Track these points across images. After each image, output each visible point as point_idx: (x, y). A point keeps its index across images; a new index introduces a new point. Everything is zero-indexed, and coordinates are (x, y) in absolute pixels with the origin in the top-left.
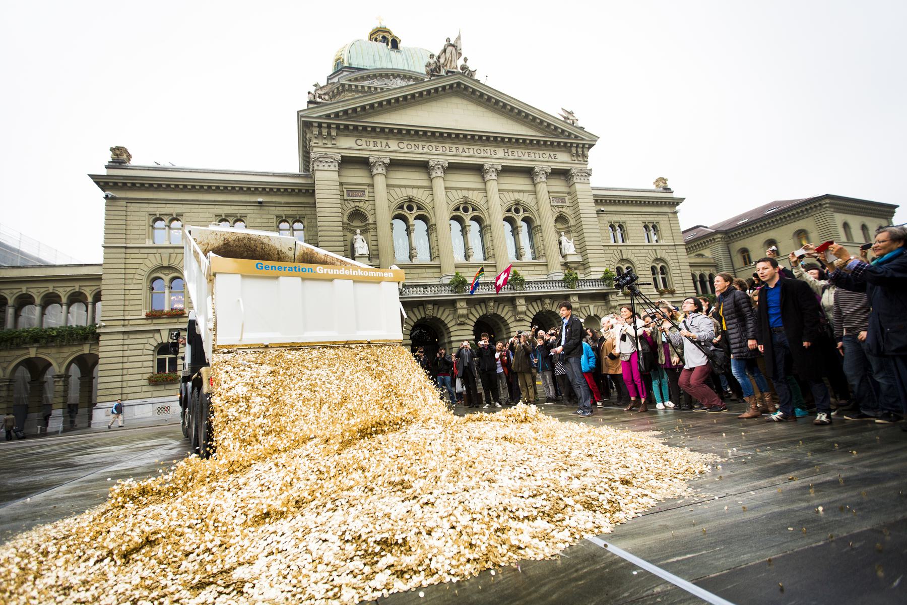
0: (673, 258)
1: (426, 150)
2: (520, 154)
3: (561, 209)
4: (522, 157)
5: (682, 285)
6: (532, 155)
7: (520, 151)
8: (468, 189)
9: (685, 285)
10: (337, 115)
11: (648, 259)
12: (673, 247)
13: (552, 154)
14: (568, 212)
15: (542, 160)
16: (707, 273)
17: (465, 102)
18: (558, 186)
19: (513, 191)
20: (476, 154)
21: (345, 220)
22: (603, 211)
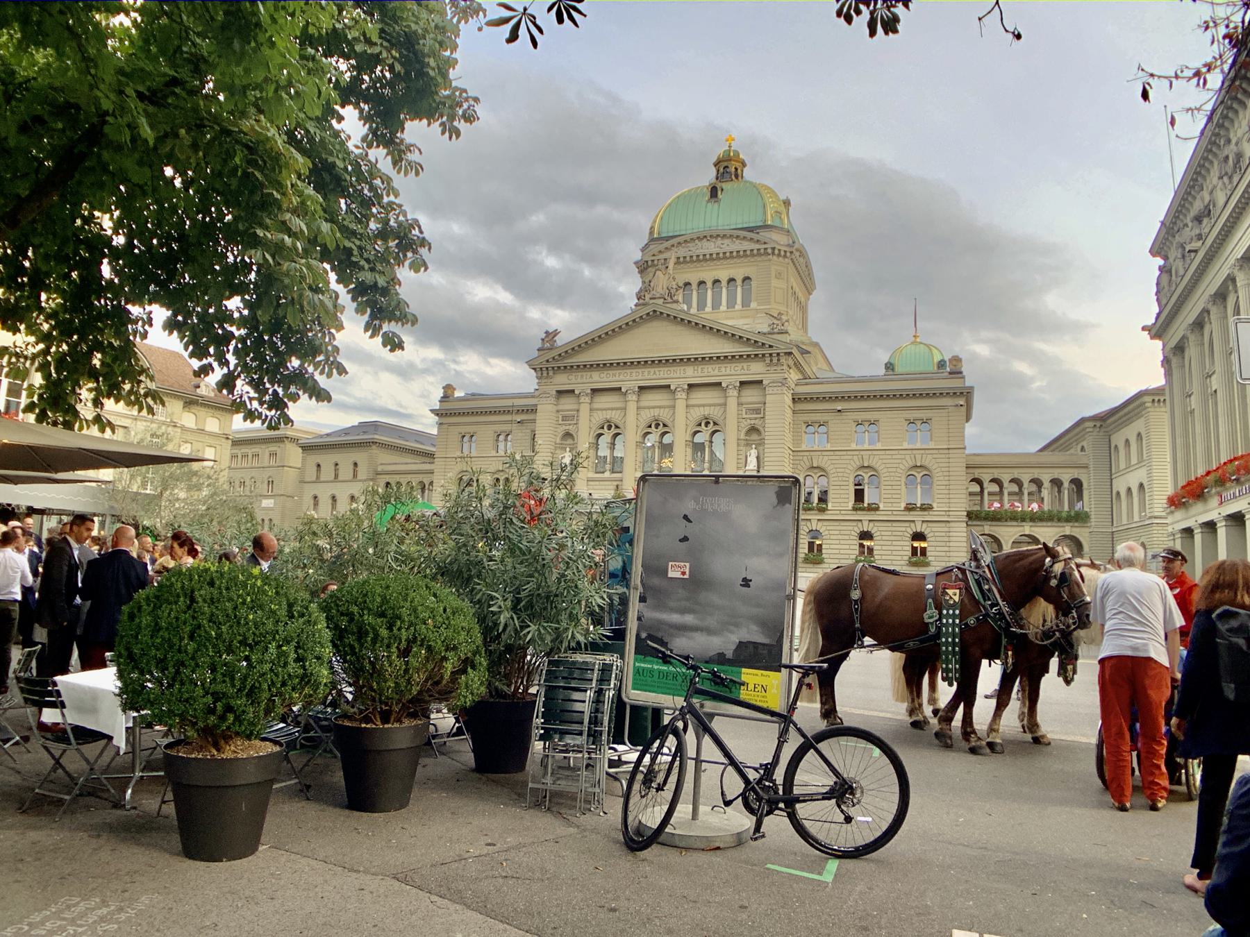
0: (941, 465)
1: (622, 377)
2: (710, 370)
3: (753, 422)
4: (712, 373)
5: (947, 501)
6: (723, 369)
7: (710, 367)
8: (660, 407)
9: (952, 501)
10: (554, 358)
11: (901, 466)
12: (947, 451)
13: (745, 365)
14: (758, 423)
15: (730, 374)
16: (1066, 478)
17: (665, 323)
18: (751, 395)
19: (704, 406)
20: (666, 376)
21: (558, 441)
22: (839, 411)
